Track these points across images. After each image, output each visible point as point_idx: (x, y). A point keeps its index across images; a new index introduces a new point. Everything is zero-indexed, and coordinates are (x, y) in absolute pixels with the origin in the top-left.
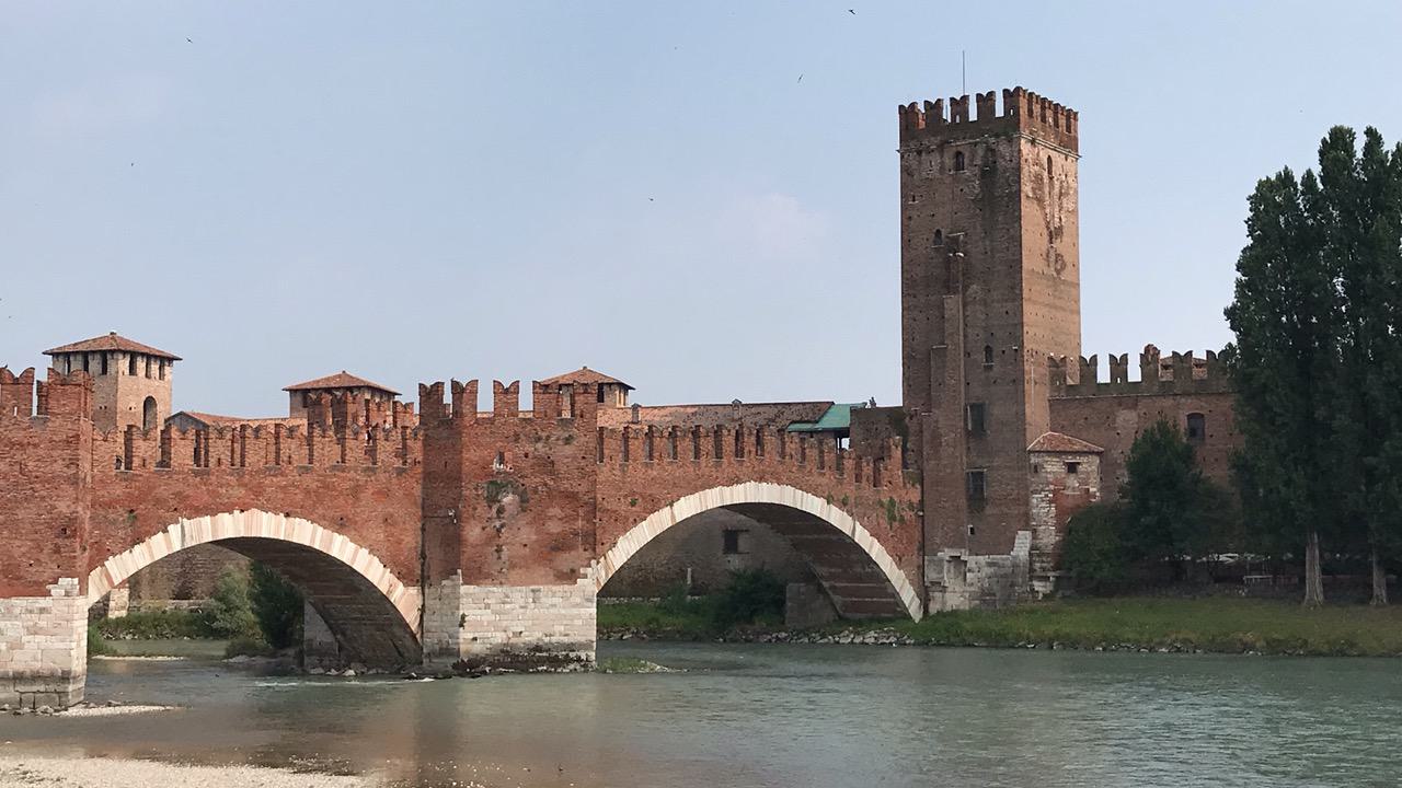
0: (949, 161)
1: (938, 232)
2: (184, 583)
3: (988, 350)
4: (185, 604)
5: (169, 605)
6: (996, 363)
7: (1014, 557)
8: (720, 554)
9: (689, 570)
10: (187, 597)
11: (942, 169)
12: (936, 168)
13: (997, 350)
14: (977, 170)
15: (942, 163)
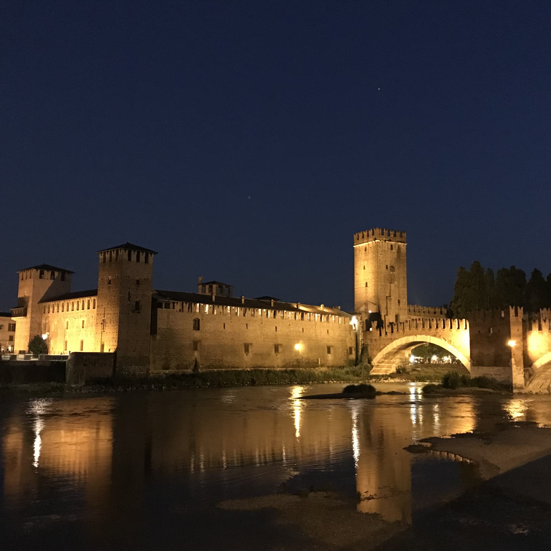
0: (390, 247)
1: (387, 266)
2: (167, 362)
3: (399, 302)
4: (167, 371)
5: (162, 372)
6: (401, 304)
7: (406, 357)
8: (326, 353)
9: (319, 359)
10: (168, 369)
11: (388, 248)
12: (386, 247)
13: (401, 301)
14: (396, 251)
15: (388, 246)
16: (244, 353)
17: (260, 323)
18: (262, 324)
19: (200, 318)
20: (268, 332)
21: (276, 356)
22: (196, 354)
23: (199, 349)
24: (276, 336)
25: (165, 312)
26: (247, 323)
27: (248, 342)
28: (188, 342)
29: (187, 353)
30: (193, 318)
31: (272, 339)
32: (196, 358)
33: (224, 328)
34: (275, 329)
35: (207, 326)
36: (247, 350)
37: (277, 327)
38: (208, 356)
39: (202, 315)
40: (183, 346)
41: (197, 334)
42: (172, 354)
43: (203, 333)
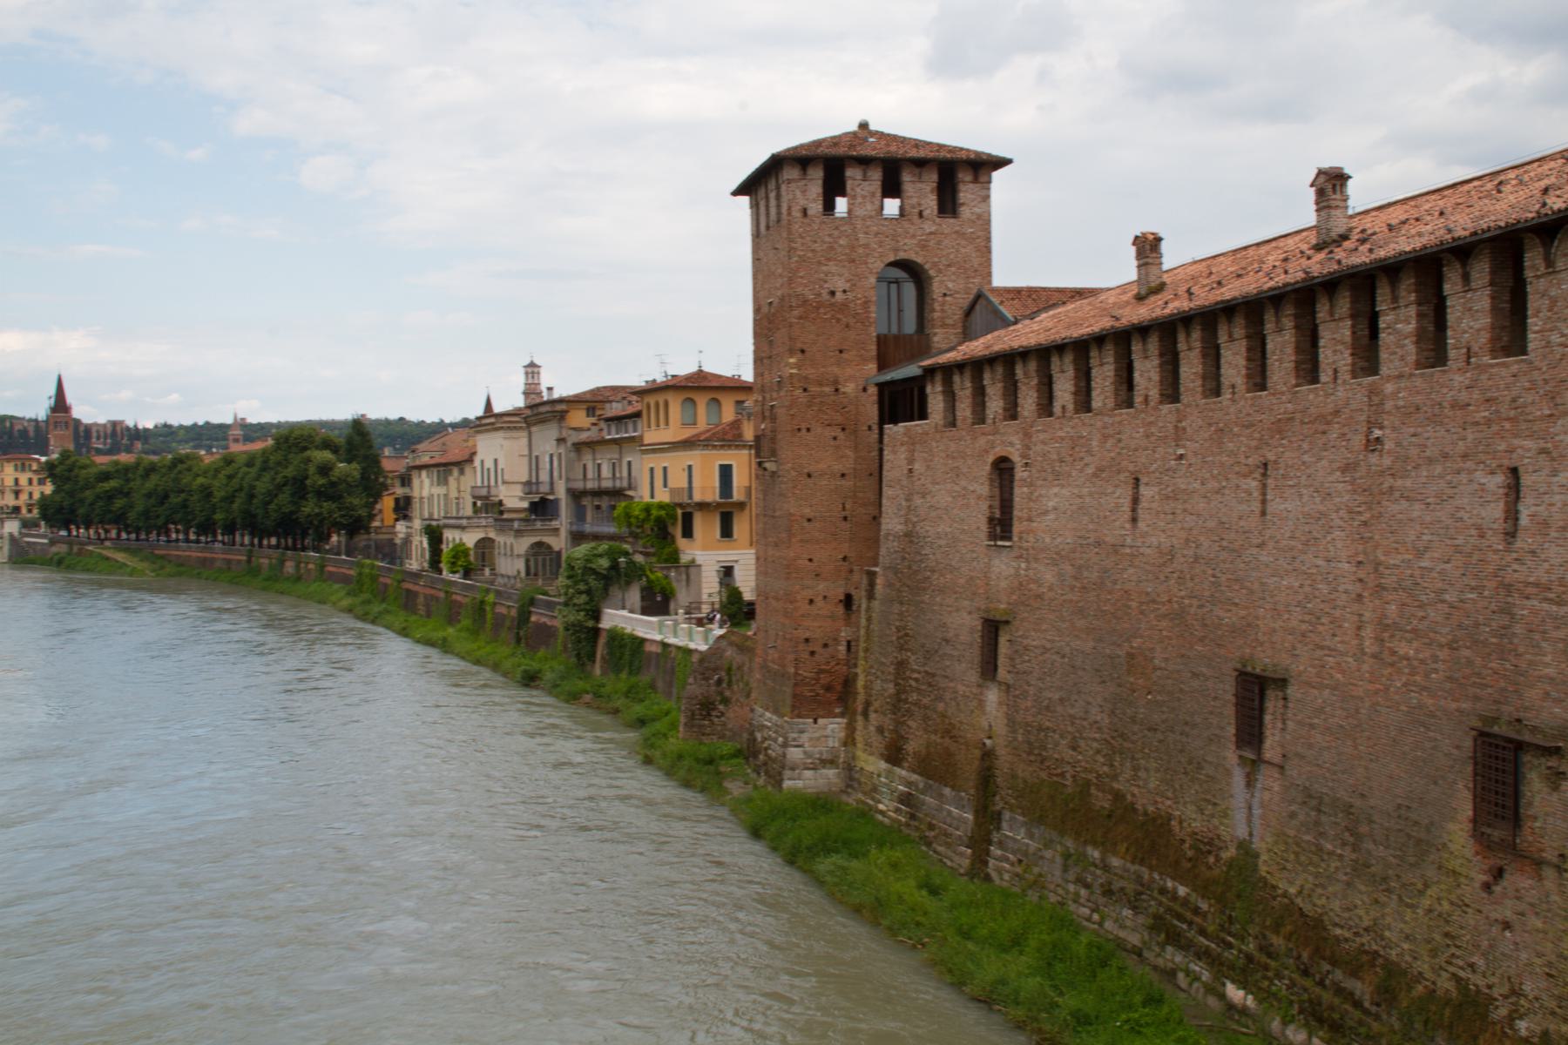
16: (1231, 755)
17: (1358, 440)
18: (1374, 459)
19: (1016, 458)
20: (1419, 554)
21: (1487, 887)
22: (992, 696)
23: (1002, 673)
24: (1507, 611)
25: (902, 444)
26: (1271, 456)
27: (1264, 660)
28: (964, 624)
29: (961, 688)
30: (991, 459)
31: (1452, 646)
32: (990, 726)
33: (1134, 520)
34: (1496, 511)
35: (1046, 513)
36: (1250, 733)
37: (1526, 480)
38: (1040, 729)
39: (1027, 435)
40: (947, 641)
41: (1003, 566)
42: (913, 683)
43: (1027, 561)
